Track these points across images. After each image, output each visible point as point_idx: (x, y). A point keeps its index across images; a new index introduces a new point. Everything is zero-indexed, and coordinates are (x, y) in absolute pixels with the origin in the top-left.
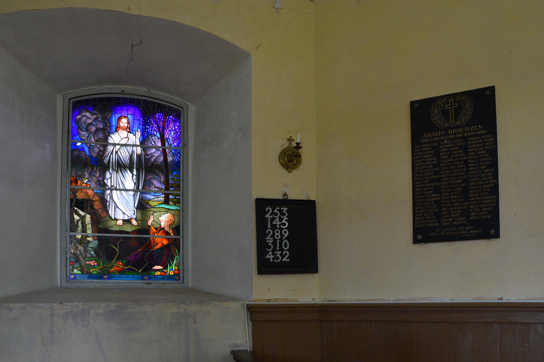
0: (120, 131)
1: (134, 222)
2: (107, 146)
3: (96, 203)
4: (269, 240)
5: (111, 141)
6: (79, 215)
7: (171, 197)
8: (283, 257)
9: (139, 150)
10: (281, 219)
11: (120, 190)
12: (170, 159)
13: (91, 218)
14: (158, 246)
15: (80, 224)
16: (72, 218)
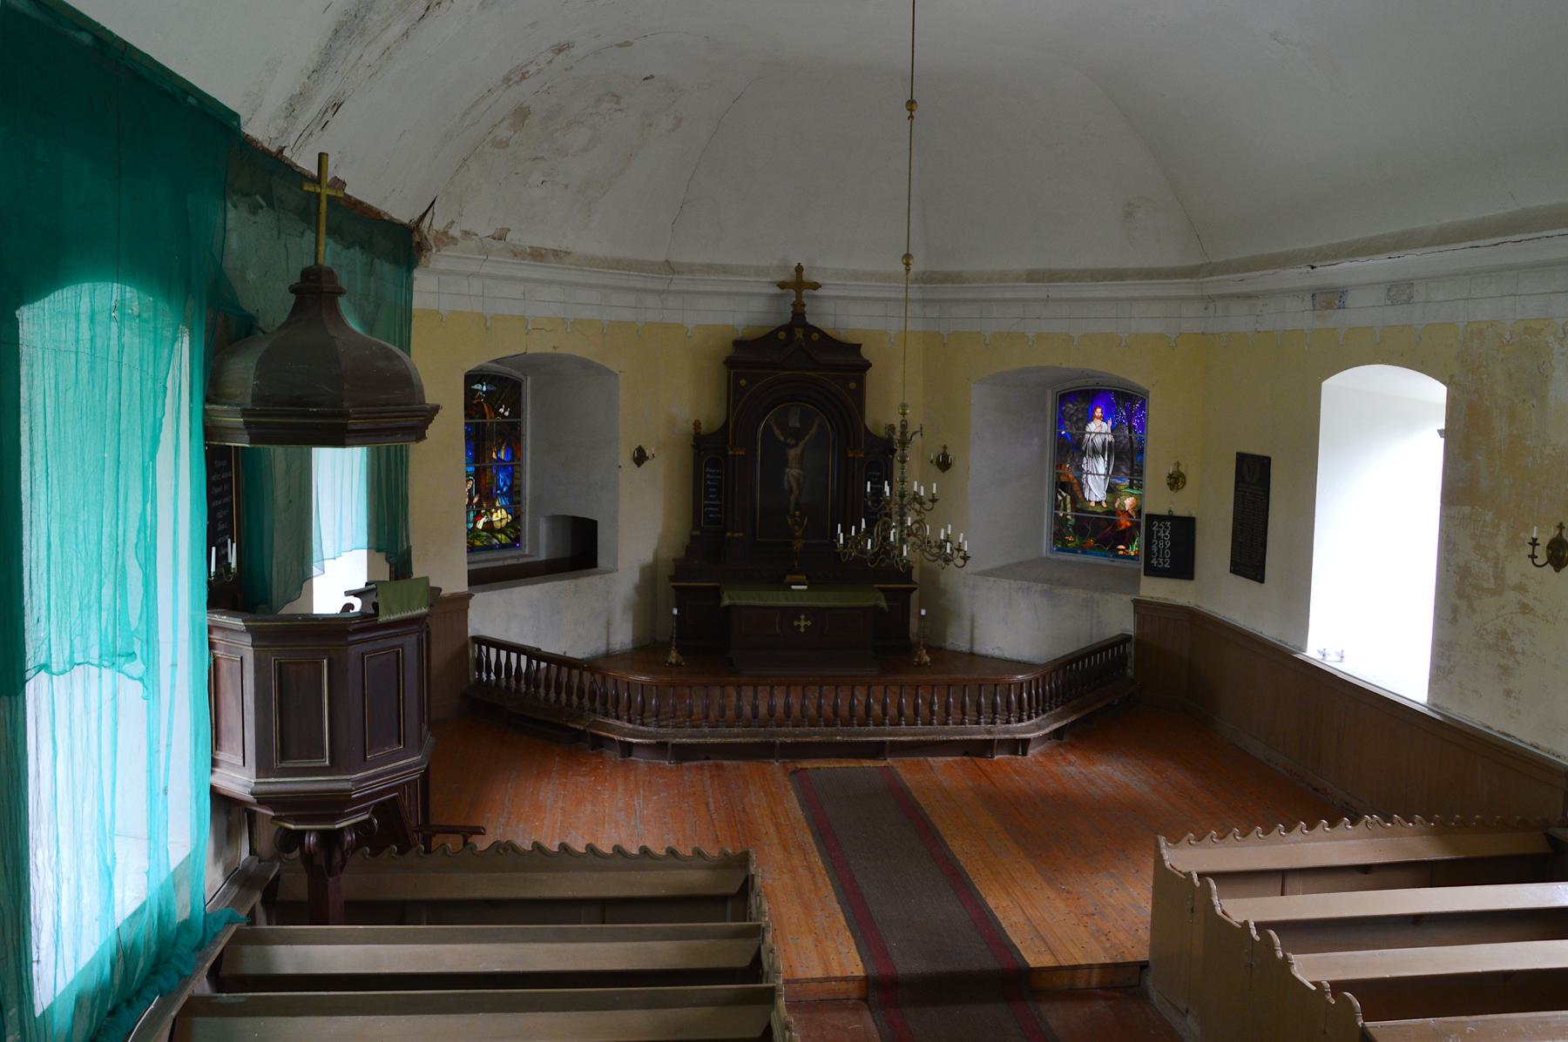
0: (1095, 420)
1: (1104, 505)
2: (1084, 434)
3: (1075, 486)
4: (1155, 549)
5: (1088, 430)
6: (1062, 496)
7: (1135, 482)
8: (1164, 563)
9: (1110, 438)
10: (1164, 532)
11: (1094, 474)
12: (1135, 446)
13: (1071, 499)
14: (1123, 527)
15: (1062, 504)
16: (1057, 498)
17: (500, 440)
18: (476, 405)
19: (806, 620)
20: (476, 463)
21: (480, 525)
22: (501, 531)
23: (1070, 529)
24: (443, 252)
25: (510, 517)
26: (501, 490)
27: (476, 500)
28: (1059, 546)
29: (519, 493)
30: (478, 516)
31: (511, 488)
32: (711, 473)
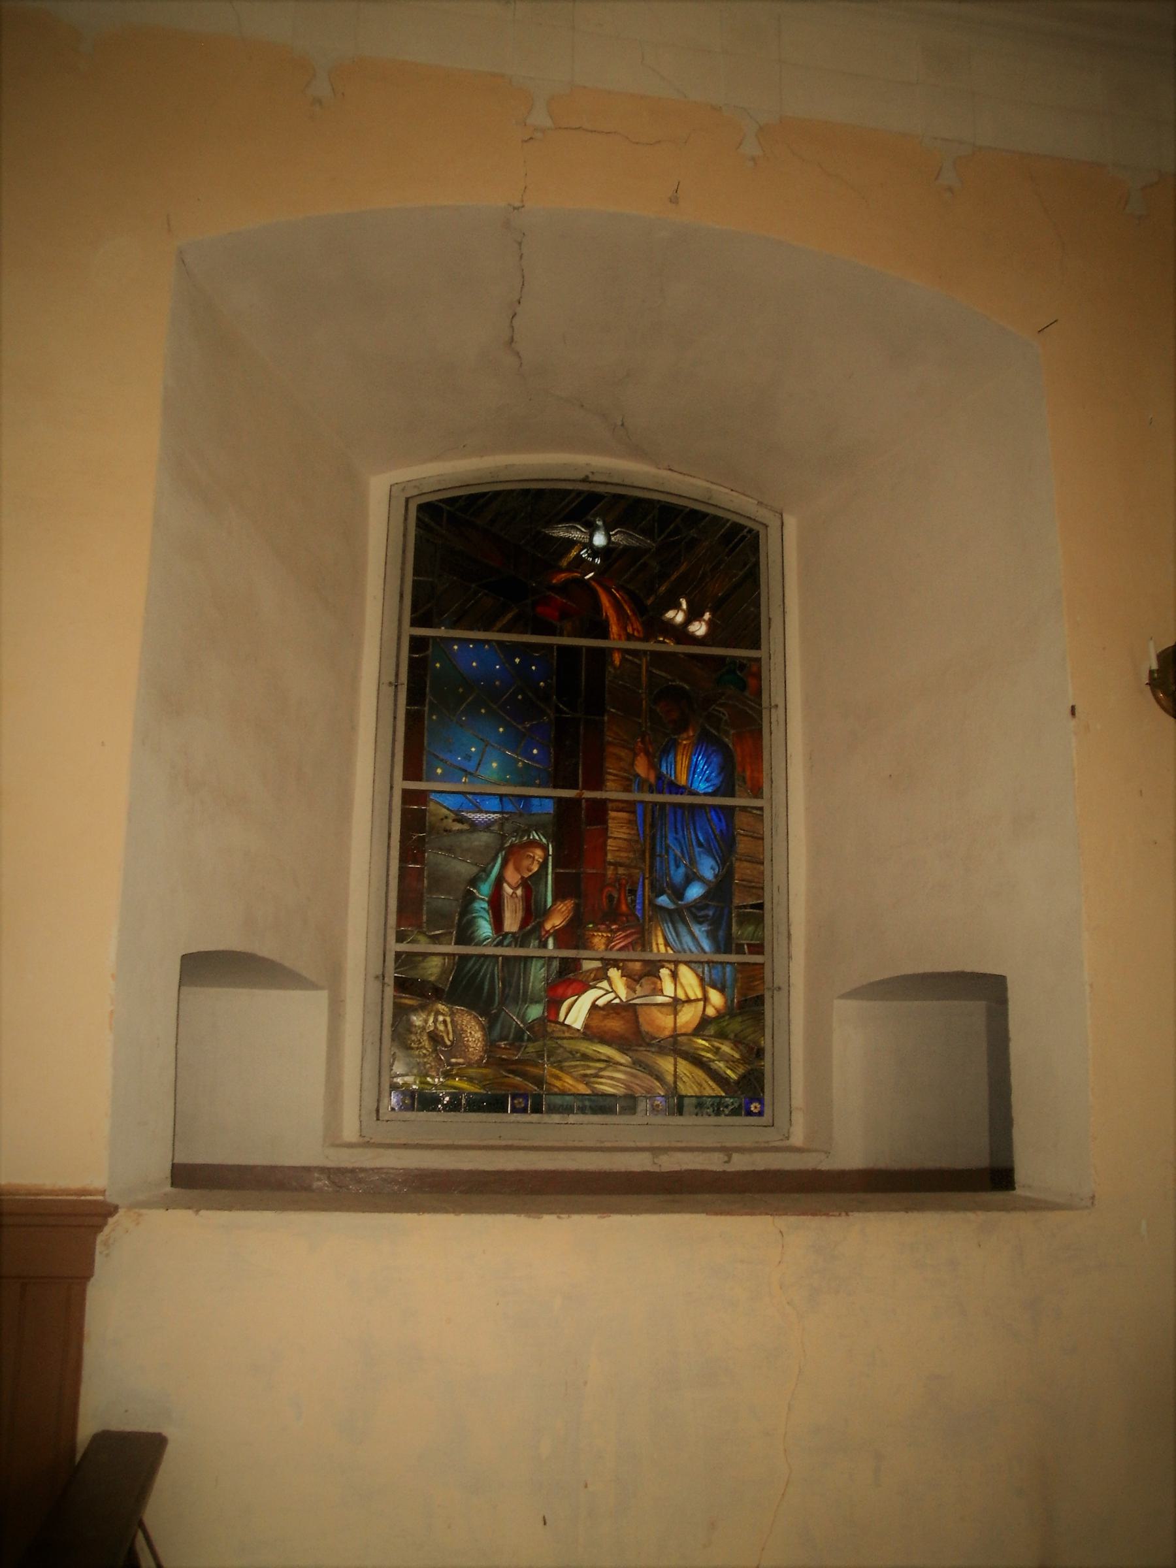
18: (564, 588)
21: (576, 1013)
22: (675, 1046)
25: (716, 997)
26: (678, 894)
29: (756, 913)
31: (720, 890)
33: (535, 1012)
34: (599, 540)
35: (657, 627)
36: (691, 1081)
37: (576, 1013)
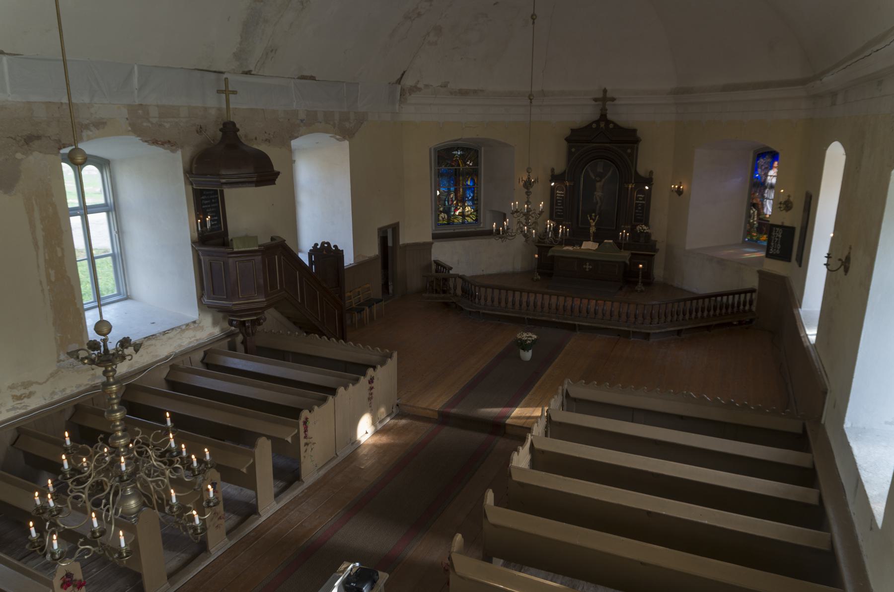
15: (753, 215)
17: (467, 177)
18: (455, 161)
19: (590, 265)
20: (456, 186)
21: (457, 213)
22: (468, 216)
23: (755, 229)
24: (412, 95)
25: (472, 210)
26: (468, 198)
27: (455, 202)
28: (749, 238)
29: (477, 200)
30: (456, 209)
31: (473, 197)
32: (559, 193)
33: (452, 213)
34: (459, 153)
35: (466, 164)
36: (470, 220)
37: (457, 213)
